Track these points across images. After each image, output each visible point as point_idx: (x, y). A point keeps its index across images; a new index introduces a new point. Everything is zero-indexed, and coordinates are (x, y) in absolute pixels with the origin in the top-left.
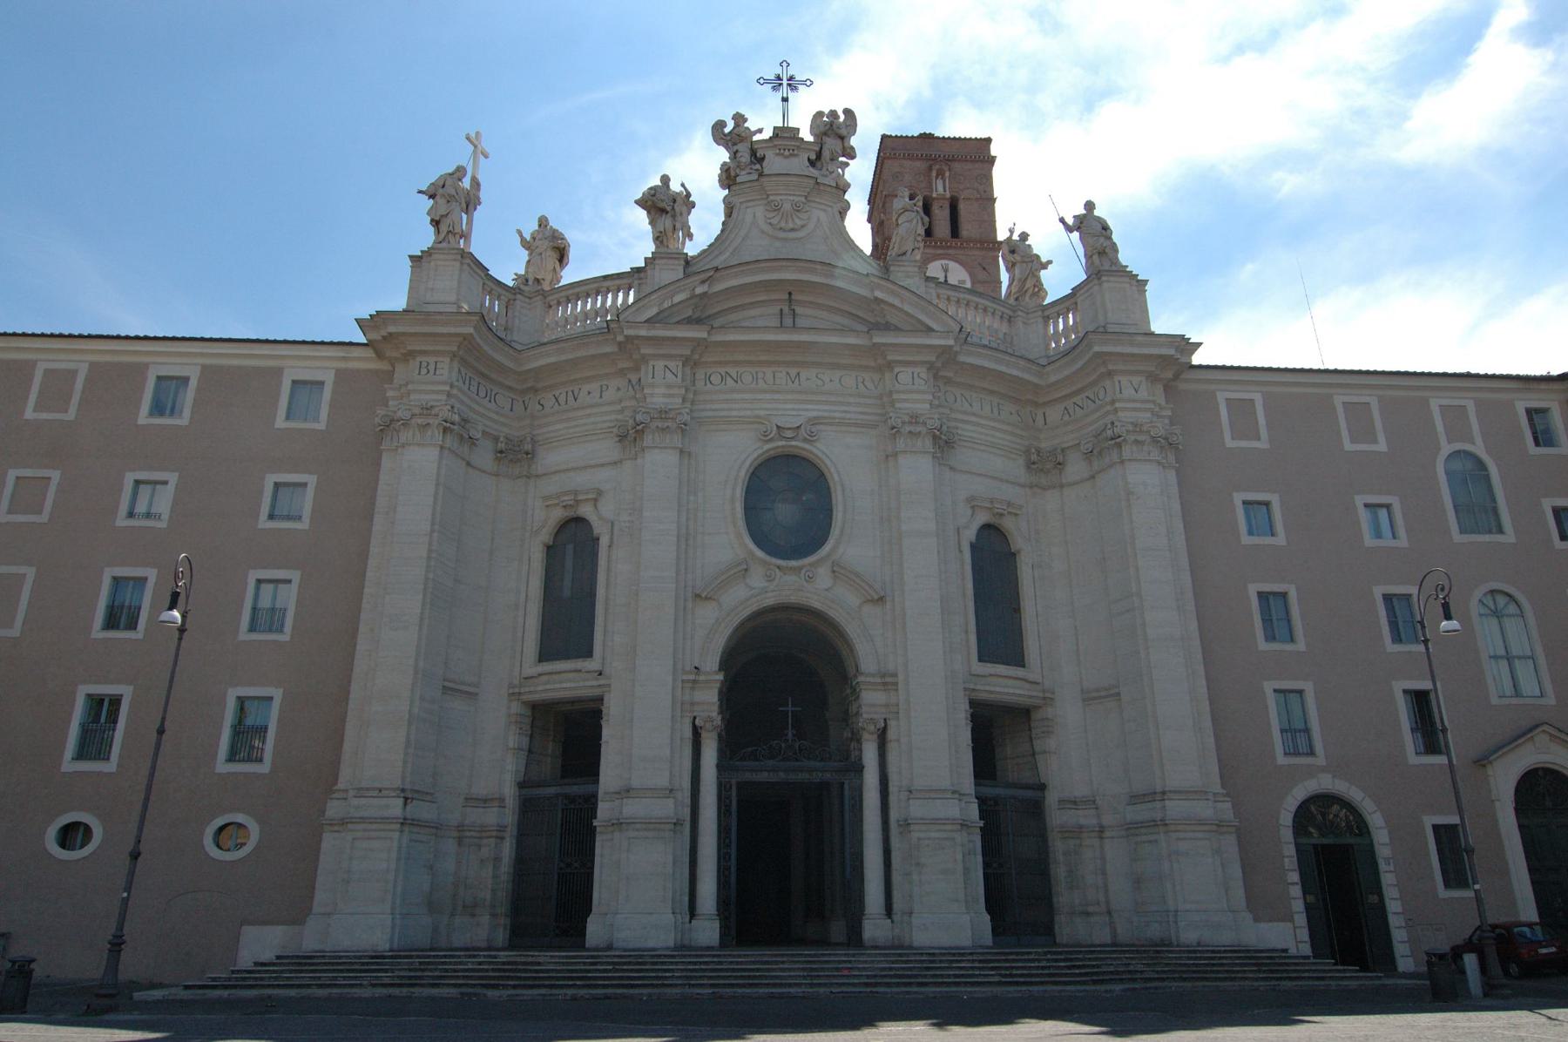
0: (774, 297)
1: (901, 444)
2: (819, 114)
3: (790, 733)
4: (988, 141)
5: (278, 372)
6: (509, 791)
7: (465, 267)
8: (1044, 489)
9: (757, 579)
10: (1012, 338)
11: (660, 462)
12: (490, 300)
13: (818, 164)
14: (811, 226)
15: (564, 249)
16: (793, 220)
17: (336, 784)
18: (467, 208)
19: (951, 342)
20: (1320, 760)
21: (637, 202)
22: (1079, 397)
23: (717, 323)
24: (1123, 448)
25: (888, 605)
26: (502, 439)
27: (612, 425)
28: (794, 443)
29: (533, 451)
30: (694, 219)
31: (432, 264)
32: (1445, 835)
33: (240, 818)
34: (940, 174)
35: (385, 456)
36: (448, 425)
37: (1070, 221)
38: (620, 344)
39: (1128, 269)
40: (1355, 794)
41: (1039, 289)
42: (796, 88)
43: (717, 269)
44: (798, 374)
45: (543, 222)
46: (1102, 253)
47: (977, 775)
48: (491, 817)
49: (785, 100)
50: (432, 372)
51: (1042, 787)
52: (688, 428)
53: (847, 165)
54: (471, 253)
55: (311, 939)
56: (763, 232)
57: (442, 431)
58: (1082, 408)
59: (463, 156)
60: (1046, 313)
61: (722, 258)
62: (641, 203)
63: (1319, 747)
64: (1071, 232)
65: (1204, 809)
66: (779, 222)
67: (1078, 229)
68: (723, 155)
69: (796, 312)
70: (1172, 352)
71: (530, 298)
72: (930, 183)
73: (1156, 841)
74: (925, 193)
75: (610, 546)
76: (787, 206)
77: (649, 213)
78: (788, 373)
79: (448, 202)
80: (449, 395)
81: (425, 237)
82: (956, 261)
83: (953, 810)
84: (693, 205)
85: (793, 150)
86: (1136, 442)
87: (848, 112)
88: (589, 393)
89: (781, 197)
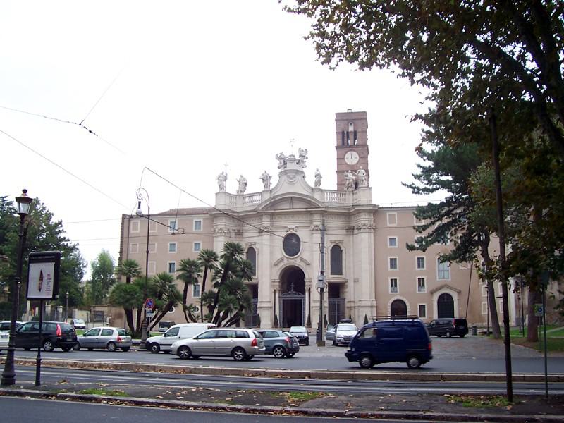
5: (192, 219)
11: (266, 237)
30: (271, 181)
32: (422, 308)
34: (351, 124)
40: (404, 300)
45: (242, 176)
51: (344, 299)
63: (398, 290)
81: (217, 190)
87: (306, 150)
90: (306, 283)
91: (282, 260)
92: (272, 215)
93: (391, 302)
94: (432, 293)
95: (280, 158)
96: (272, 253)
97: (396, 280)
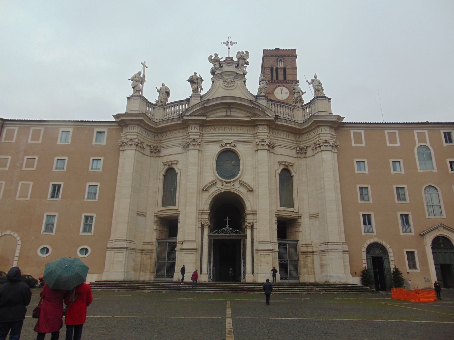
0: (225, 106)
1: (259, 147)
2: (239, 53)
3: (227, 226)
4: (295, 50)
6: (154, 241)
7: (141, 100)
8: (302, 158)
9: (219, 185)
10: (293, 115)
11: (193, 154)
12: (148, 108)
13: (238, 67)
14: (235, 86)
15: (169, 92)
16: (230, 84)
17: (110, 238)
18: (142, 82)
19: (273, 119)
20: (375, 234)
21: (187, 81)
22: (311, 132)
23: (209, 114)
24: (321, 147)
25: (255, 192)
26: (152, 146)
27: (181, 142)
28: (230, 147)
29: (160, 149)
30: (203, 85)
31: (133, 99)
32: (411, 255)
33: (86, 247)
34: (281, 60)
35: (121, 153)
36: (137, 144)
37: (310, 81)
38: (182, 121)
39: (325, 95)
40: (384, 243)
41: (301, 101)
42: (232, 45)
43: (208, 100)
44: (231, 128)
45: (163, 85)
46: (318, 90)
47: (278, 237)
48: (149, 247)
49: (229, 48)
50: (133, 129)
51: (298, 241)
52: (200, 144)
53: (246, 67)
54: (143, 96)
55: (104, 278)
56: (222, 88)
57: (135, 145)
58: (312, 135)
59: (140, 68)
60: (304, 107)
61: (211, 96)
62: (188, 81)
63: (374, 230)
64: (310, 84)
65: (340, 247)
66: (226, 85)
67: (312, 83)
68: (212, 65)
69: (231, 110)
70: (336, 120)
71: (159, 107)
72: (278, 64)
73: (326, 255)
74: (276, 67)
75: (180, 176)
76: (229, 80)
77: (191, 83)
78: (228, 128)
79: (137, 82)
80: (137, 136)
81: (131, 92)
82: (286, 87)
83: (270, 247)
84: (203, 80)
85: (231, 64)
86: (325, 145)
87: (247, 52)
88: (175, 134)
89: (228, 78)
90: (248, 217)
91: (214, 184)
92: (203, 125)
93: (366, 246)
94: (422, 235)
95: (215, 60)
96: (200, 175)
97: (369, 216)
